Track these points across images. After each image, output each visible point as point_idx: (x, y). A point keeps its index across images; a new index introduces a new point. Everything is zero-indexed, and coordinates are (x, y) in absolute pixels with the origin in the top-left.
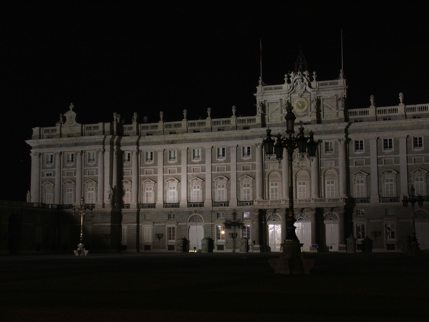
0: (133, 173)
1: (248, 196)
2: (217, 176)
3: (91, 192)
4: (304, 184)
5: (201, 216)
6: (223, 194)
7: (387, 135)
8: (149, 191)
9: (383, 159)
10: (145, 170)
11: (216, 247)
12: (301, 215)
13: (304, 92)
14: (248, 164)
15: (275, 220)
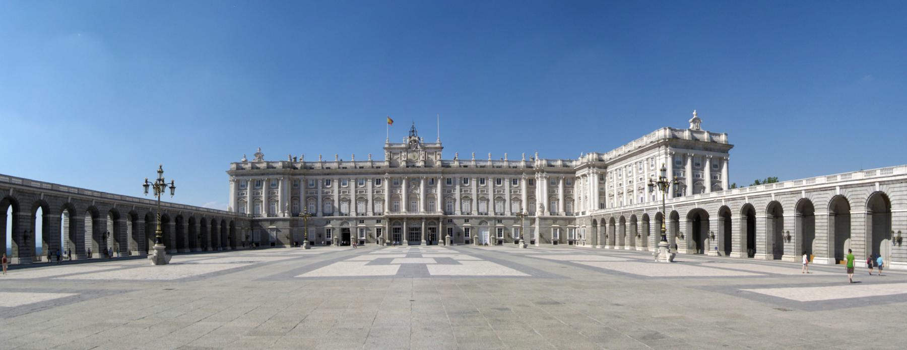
8: (312, 205)
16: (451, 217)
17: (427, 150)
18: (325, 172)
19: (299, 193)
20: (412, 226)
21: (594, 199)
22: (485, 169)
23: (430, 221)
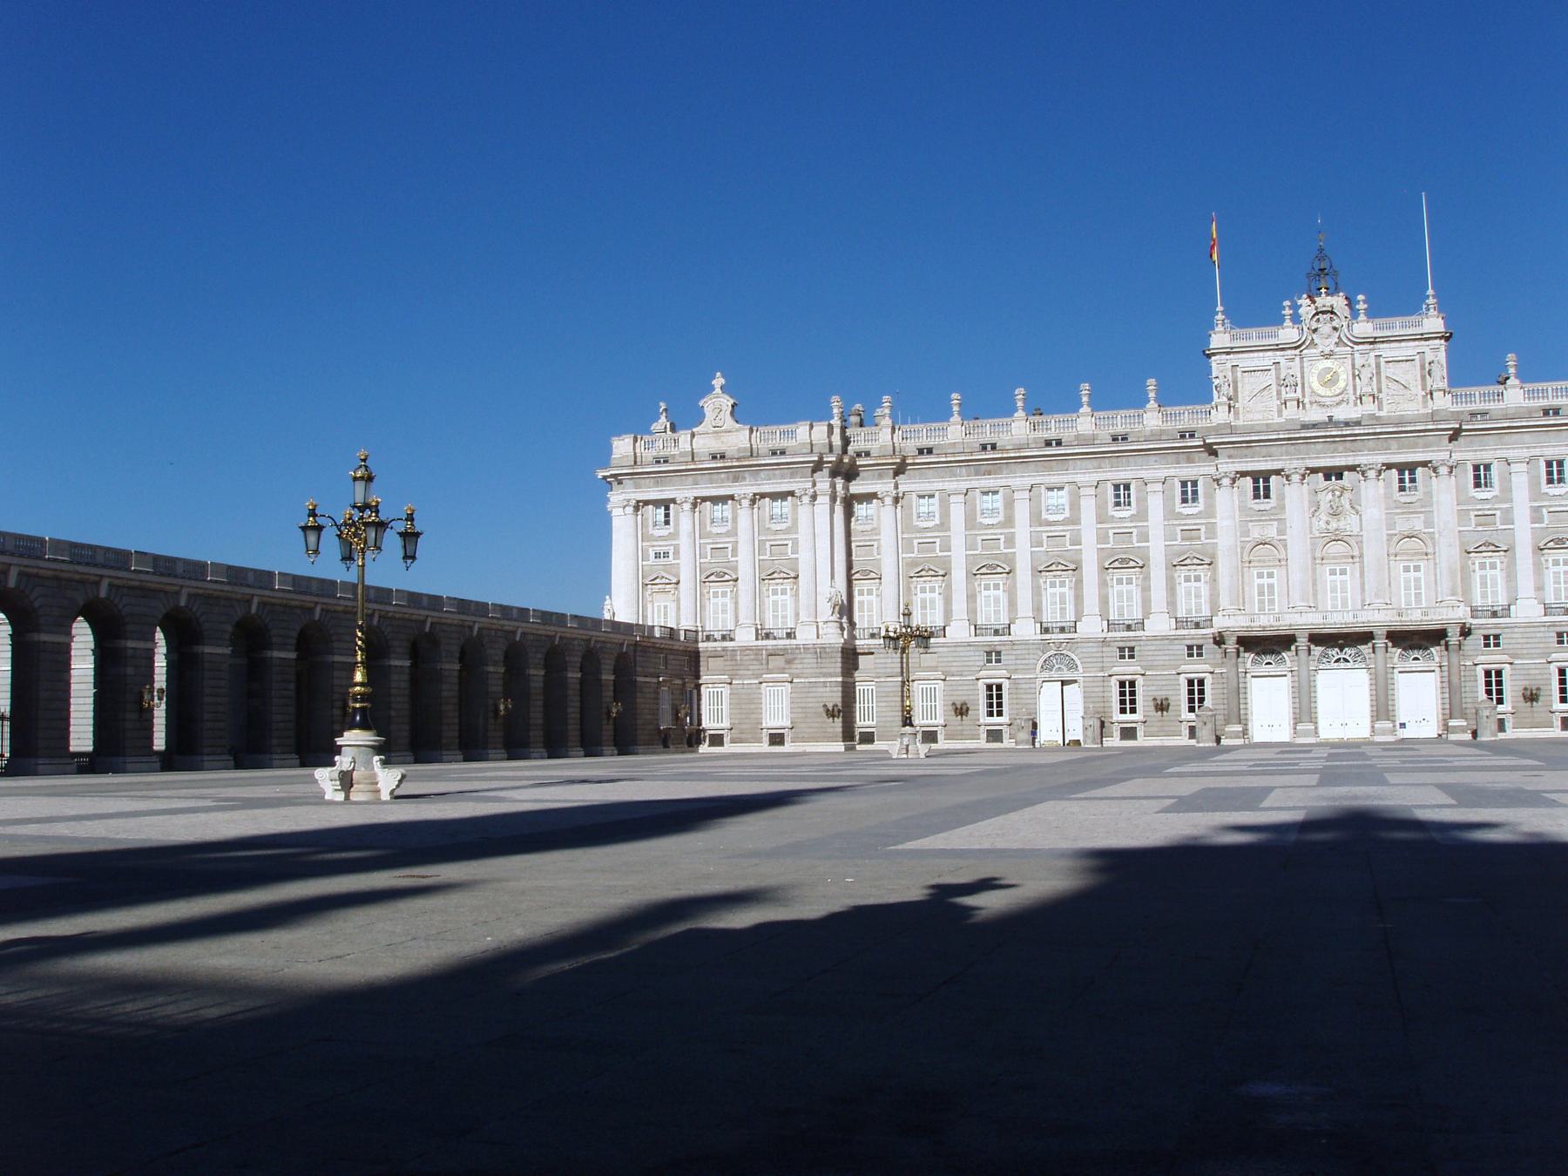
0: (883, 550)
1: (1198, 605)
2: (1112, 556)
3: (779, 597)
4: (1343, 572)
5: (1073, 656)
6: (1130, 599)
8: (928, 595)
9: (1545, 511)
10: (916, 542)
11: (1117, 734)
12: (1341, 651)
14: (1195, 524)
15: (1270, 664)
16: (1496, 626)
17: (1387, 351)
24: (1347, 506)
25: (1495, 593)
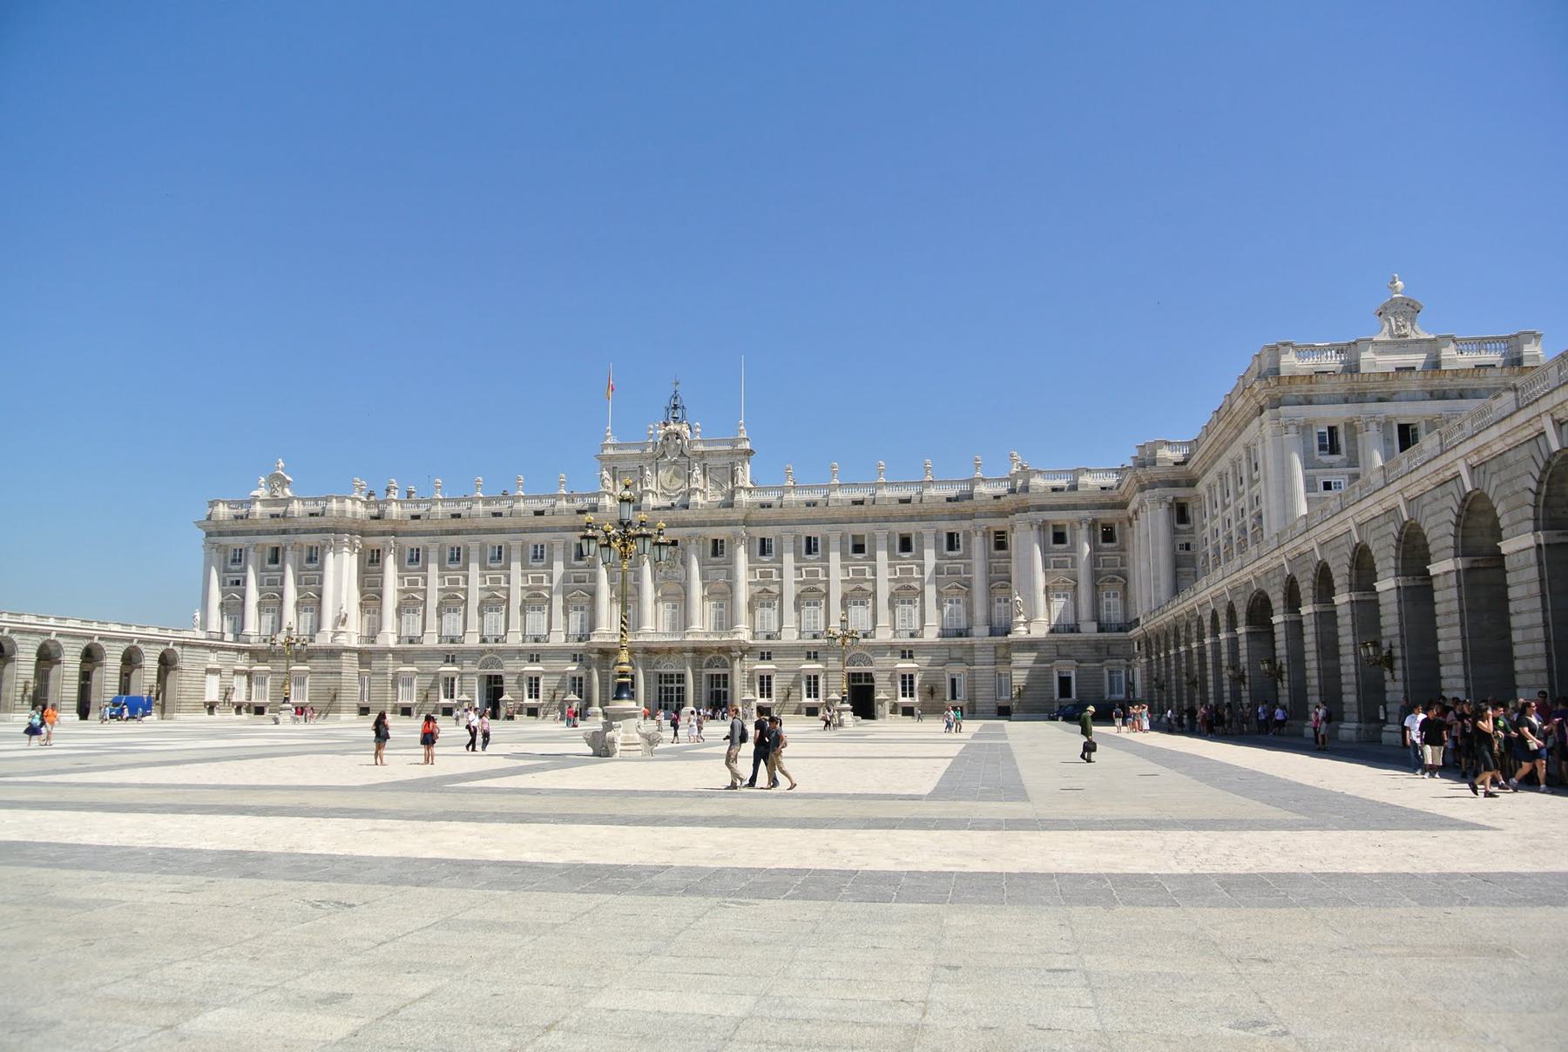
7: (810, 531)
9: (803, 569)
13: (680, 456)
16: (768, 646)
17: (710, 461)
18: (445, 527)
19: (382, 581)
20: (663, 670)
21: (1157, 578)
22: (862, 508)
23: (711, 656)
24: (679, 562)
25: (769, 624)
